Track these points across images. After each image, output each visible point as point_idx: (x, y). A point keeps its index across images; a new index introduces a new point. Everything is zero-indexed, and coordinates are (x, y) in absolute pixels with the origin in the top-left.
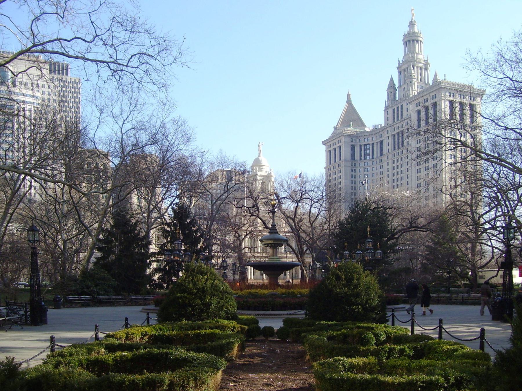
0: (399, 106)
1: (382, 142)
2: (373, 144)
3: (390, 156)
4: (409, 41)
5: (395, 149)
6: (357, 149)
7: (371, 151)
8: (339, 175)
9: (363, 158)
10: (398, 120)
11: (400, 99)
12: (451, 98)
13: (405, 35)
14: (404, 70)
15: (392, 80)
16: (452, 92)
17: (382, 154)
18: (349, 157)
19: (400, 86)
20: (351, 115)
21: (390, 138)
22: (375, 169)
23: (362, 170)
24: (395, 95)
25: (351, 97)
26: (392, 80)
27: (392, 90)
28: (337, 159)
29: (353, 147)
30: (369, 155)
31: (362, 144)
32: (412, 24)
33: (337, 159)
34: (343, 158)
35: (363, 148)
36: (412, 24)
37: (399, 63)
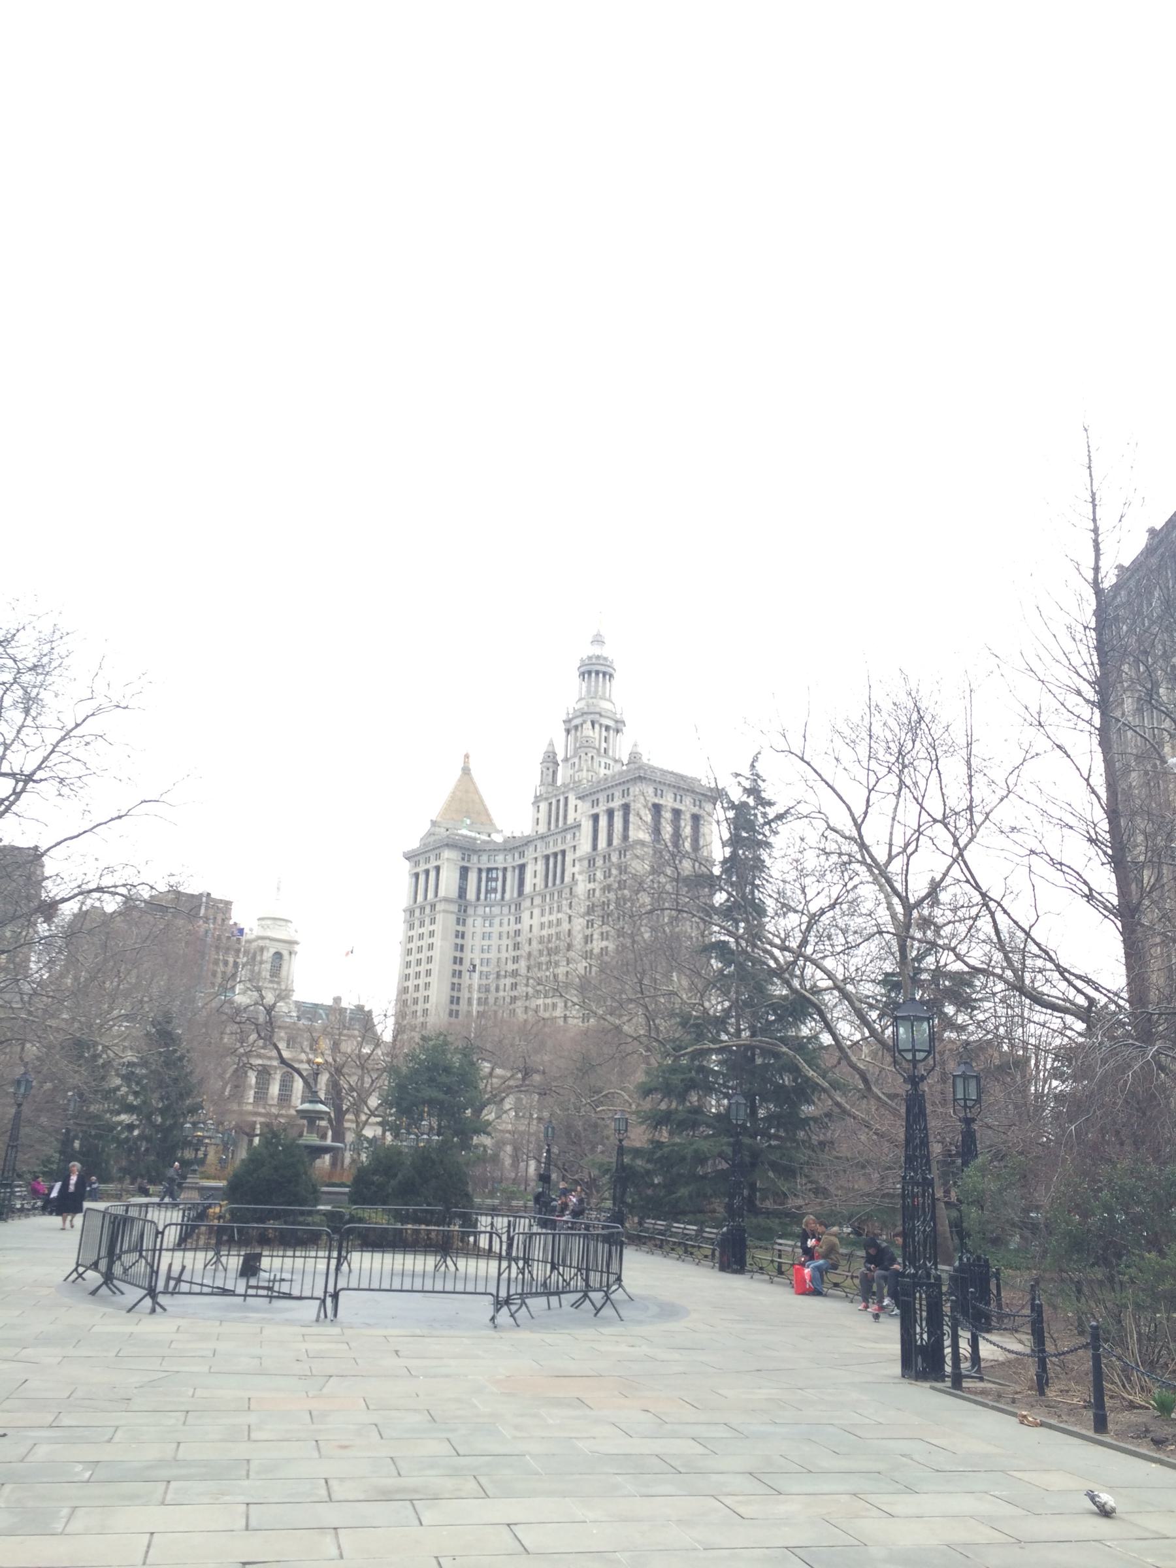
0: (562, 798)
1: (522, 867)
2: (505, 869)
3: (537, 901)
4: (590, 673)
5: (546, 886)
6: (472, 877)
7: (500, 883)
8: (431, 928)
9: (482, 896)
10: (557, 826)
13: (582, 660)
14: (576, 727)
15: (551, 744)
17: (521, 892)
18: (454, 893)
19: (566, 760)
20: (466, 799)
21: (539, 862)
22: (505, 921)
23: (479, 921)
24: (555, 773)
25: (471, 759)
26: (551, 744)
27: (550, 765)
28: (431, 895)
29: (464, 871)
30: (495, 890)
31: (484, 866)
33: (431, 895)
34: (442, 893)
35: (484, 875)
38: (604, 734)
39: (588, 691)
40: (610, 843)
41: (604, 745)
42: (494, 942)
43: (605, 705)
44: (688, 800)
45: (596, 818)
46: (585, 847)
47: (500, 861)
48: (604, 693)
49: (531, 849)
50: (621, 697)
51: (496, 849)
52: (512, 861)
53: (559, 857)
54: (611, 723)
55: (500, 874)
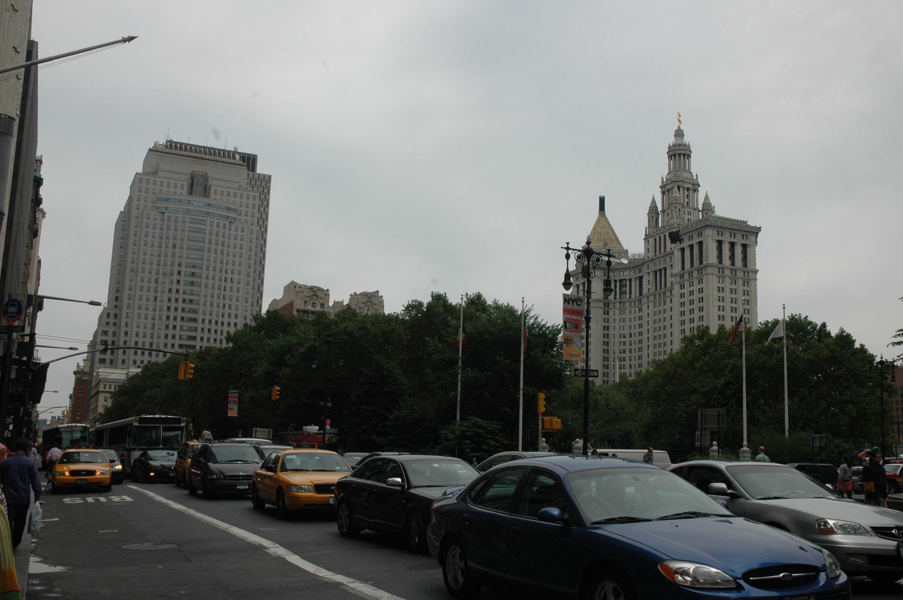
1: (641, 278)
4: (675, 155)
9: (618, 297)
11: (663, 227)
12: (720, 238)
13: (669, 147)
14: (669, 190)
15: (654, 201)
16: (720, 230)
17: (641, 294)
19: (663, 211)
23: (617, 312)
24: (657, 220)
26: (654, 201)
27: (654, 215)
32: (679, 133)
35: (618, 284)
36: (679, 133)
37: (663, 182)
38: (686, 193)
39: (675, 167)
40: (692, 266)
41: (686, 200)
42: (627, 324)
43: (686, 175)
44: (739, 236)
45: (683, 250)
46: (677, 269)
47: (626, 275)
48: (685, 167)
49: (645, 267)
50: (697, 166)
51: (625, 268)
52: (633, 275)
53: (663, 272)
54: (690, 186)
55: (628, 283)
